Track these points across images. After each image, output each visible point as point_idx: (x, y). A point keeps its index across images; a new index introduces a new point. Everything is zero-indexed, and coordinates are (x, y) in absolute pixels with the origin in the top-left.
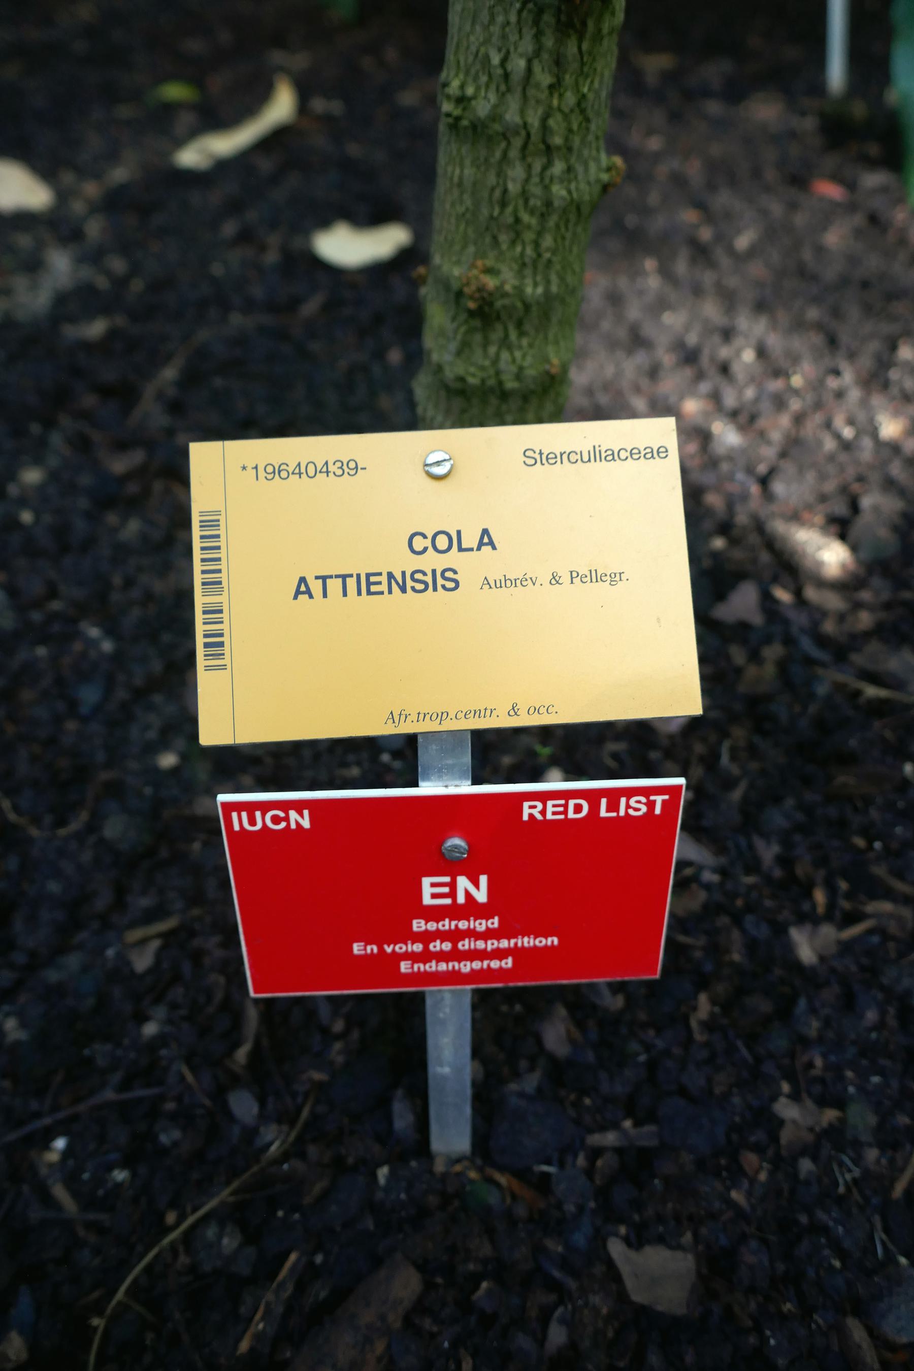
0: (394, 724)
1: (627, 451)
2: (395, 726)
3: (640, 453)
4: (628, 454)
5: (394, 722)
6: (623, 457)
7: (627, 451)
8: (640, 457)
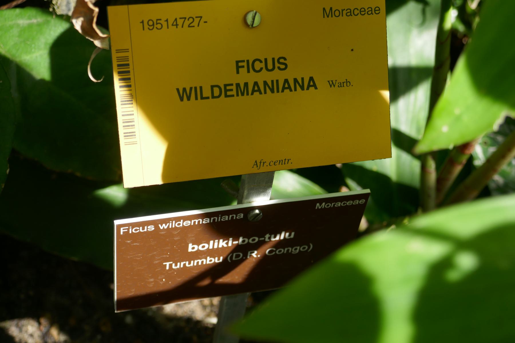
0: (257, 168)
1: (358, 10)
2: (258, 169)
3: (365, 11)
4: (359, 12)
5: (257, 167)
6: (356, 13)
7: (358, 10)
8: (365, 13)
